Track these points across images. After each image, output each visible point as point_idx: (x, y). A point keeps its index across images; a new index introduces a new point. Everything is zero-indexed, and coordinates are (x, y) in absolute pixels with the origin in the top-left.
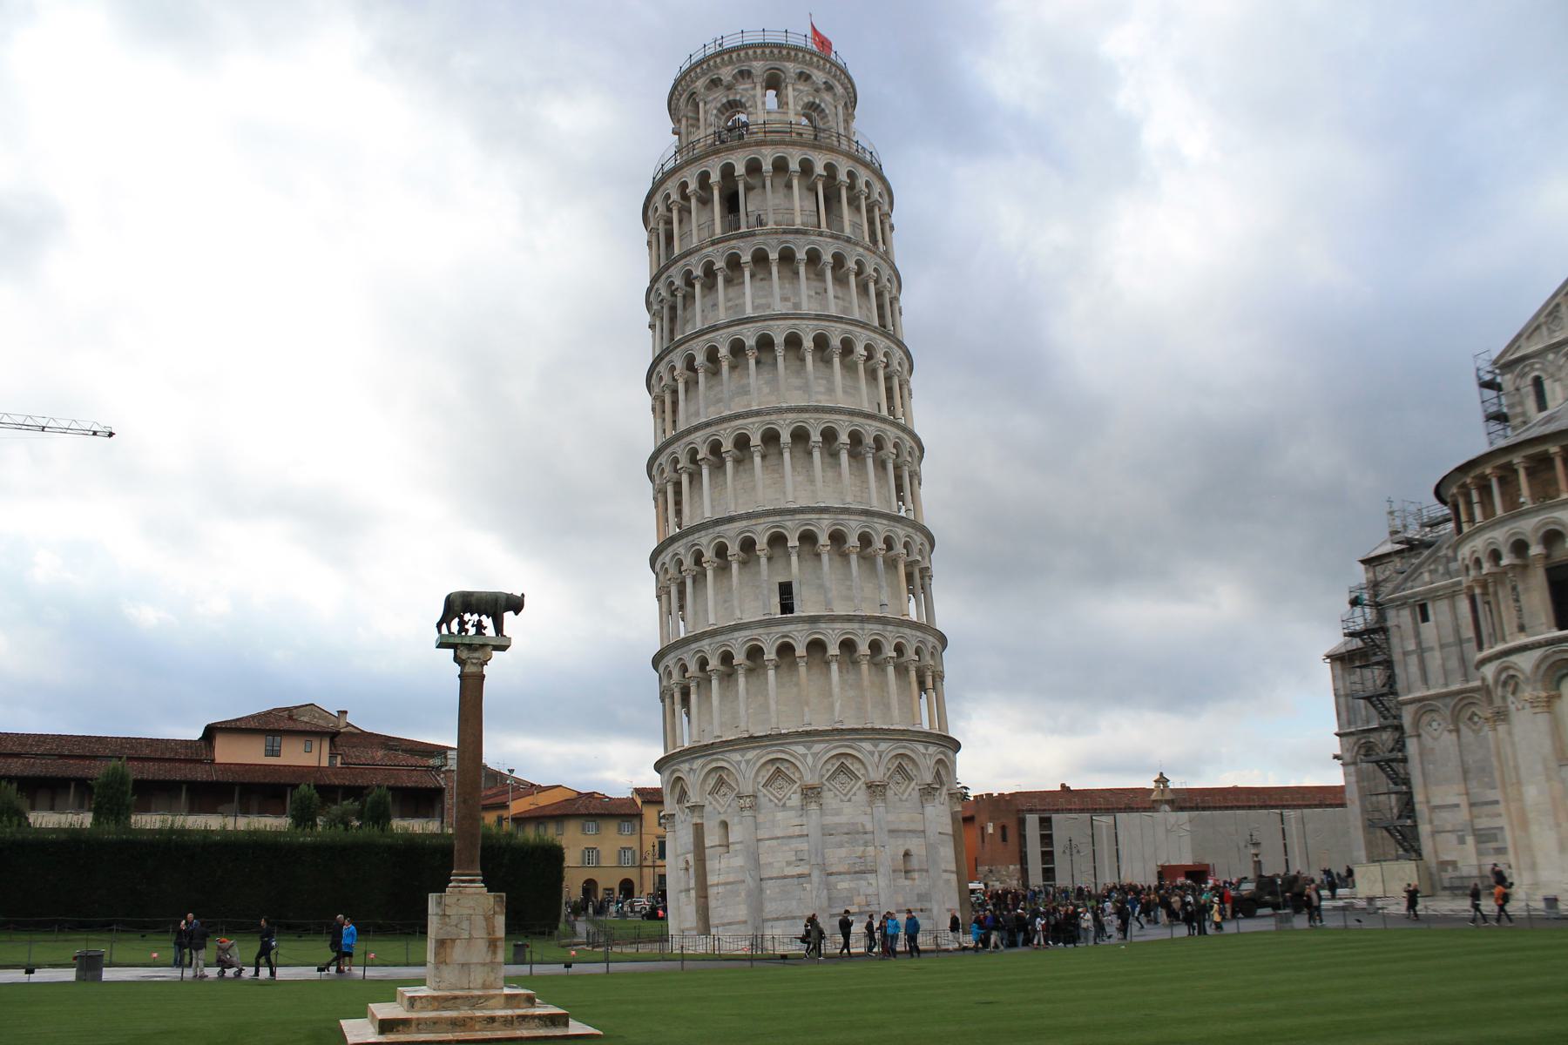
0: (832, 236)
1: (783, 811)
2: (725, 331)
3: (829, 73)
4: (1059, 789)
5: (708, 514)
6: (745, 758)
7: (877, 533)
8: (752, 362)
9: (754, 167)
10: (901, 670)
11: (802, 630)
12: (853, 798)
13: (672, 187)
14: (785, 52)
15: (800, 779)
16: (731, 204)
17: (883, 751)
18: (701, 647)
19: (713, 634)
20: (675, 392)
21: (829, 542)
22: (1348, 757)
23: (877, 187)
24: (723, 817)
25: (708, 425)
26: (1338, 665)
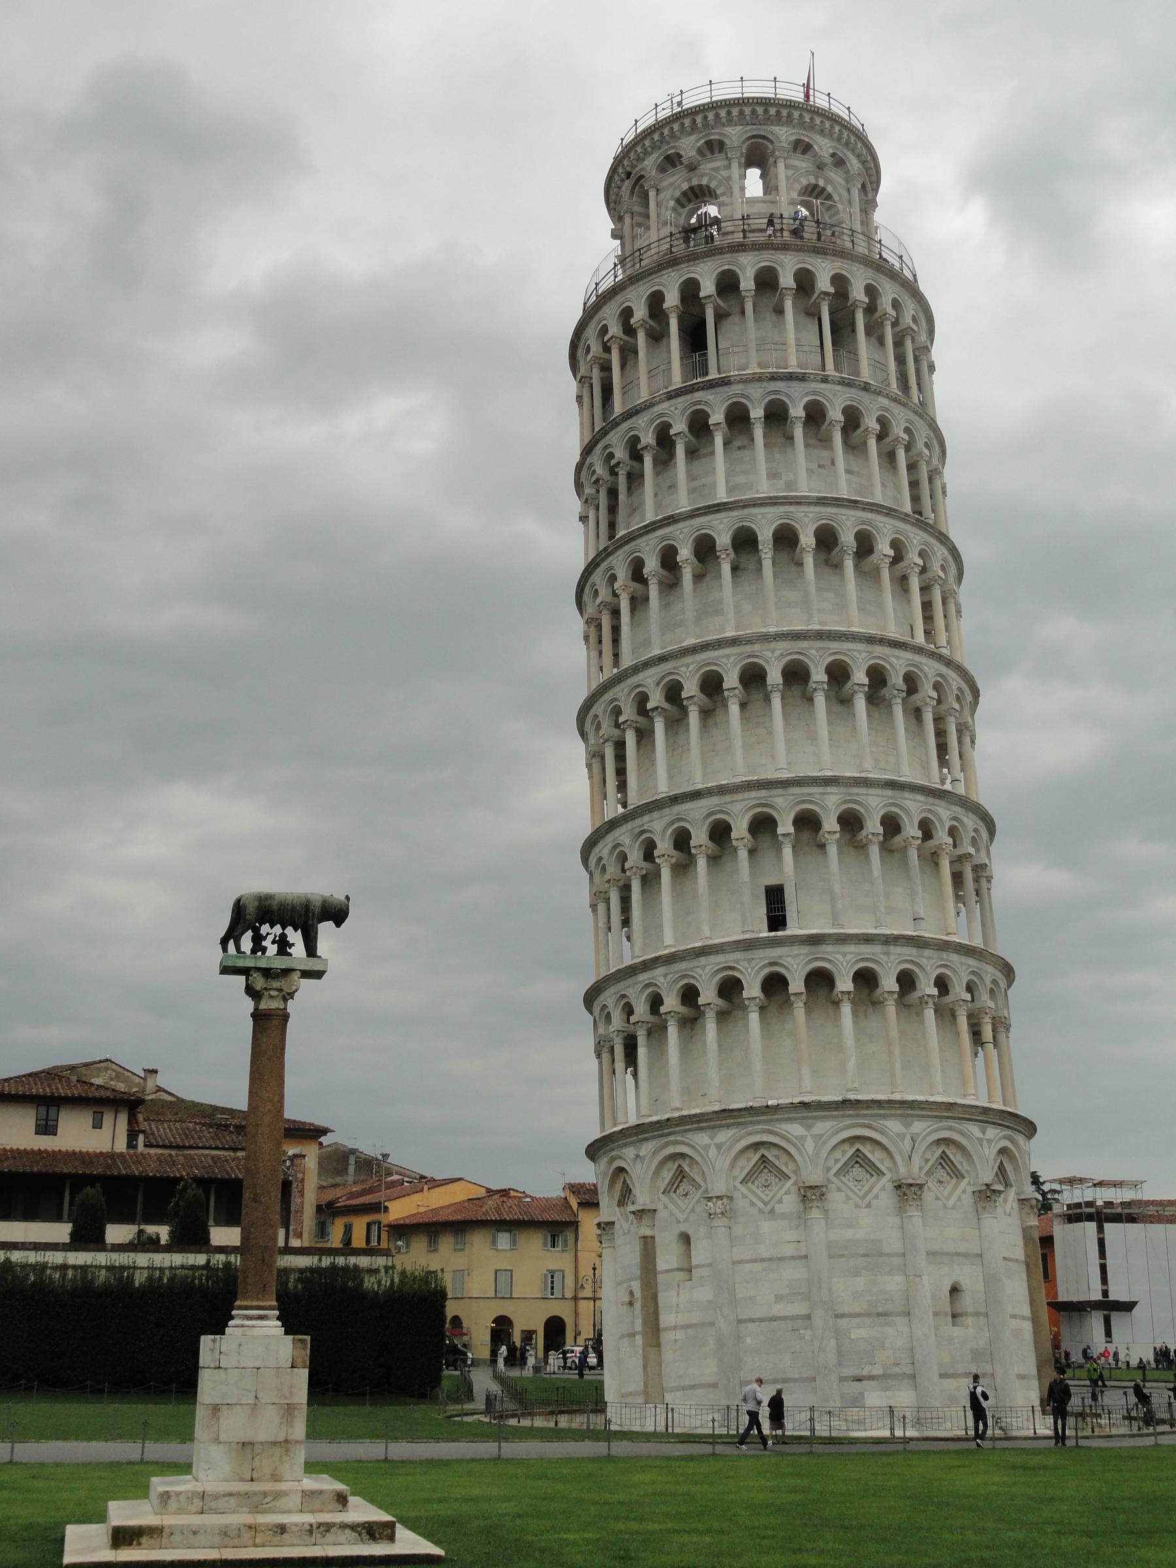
0: (843, 383)
1: (769, 1220)
3: (839, 139)
5: (663, 789)
8: (726, 568)
9: (728, 285)
10: (946, 1015)
11: (799, 955)
12: (874, 1202)
13: (610, 316)
14: (772, 111)
15: (795, 1172)
16: (695, 339)
17: (918, 1135)
18: (653, 978)
19: (671, 959)
20: (616, 613)
21: (837, 827)
23: (910, 308)
24: (683, 1228)
25: (662, 659)
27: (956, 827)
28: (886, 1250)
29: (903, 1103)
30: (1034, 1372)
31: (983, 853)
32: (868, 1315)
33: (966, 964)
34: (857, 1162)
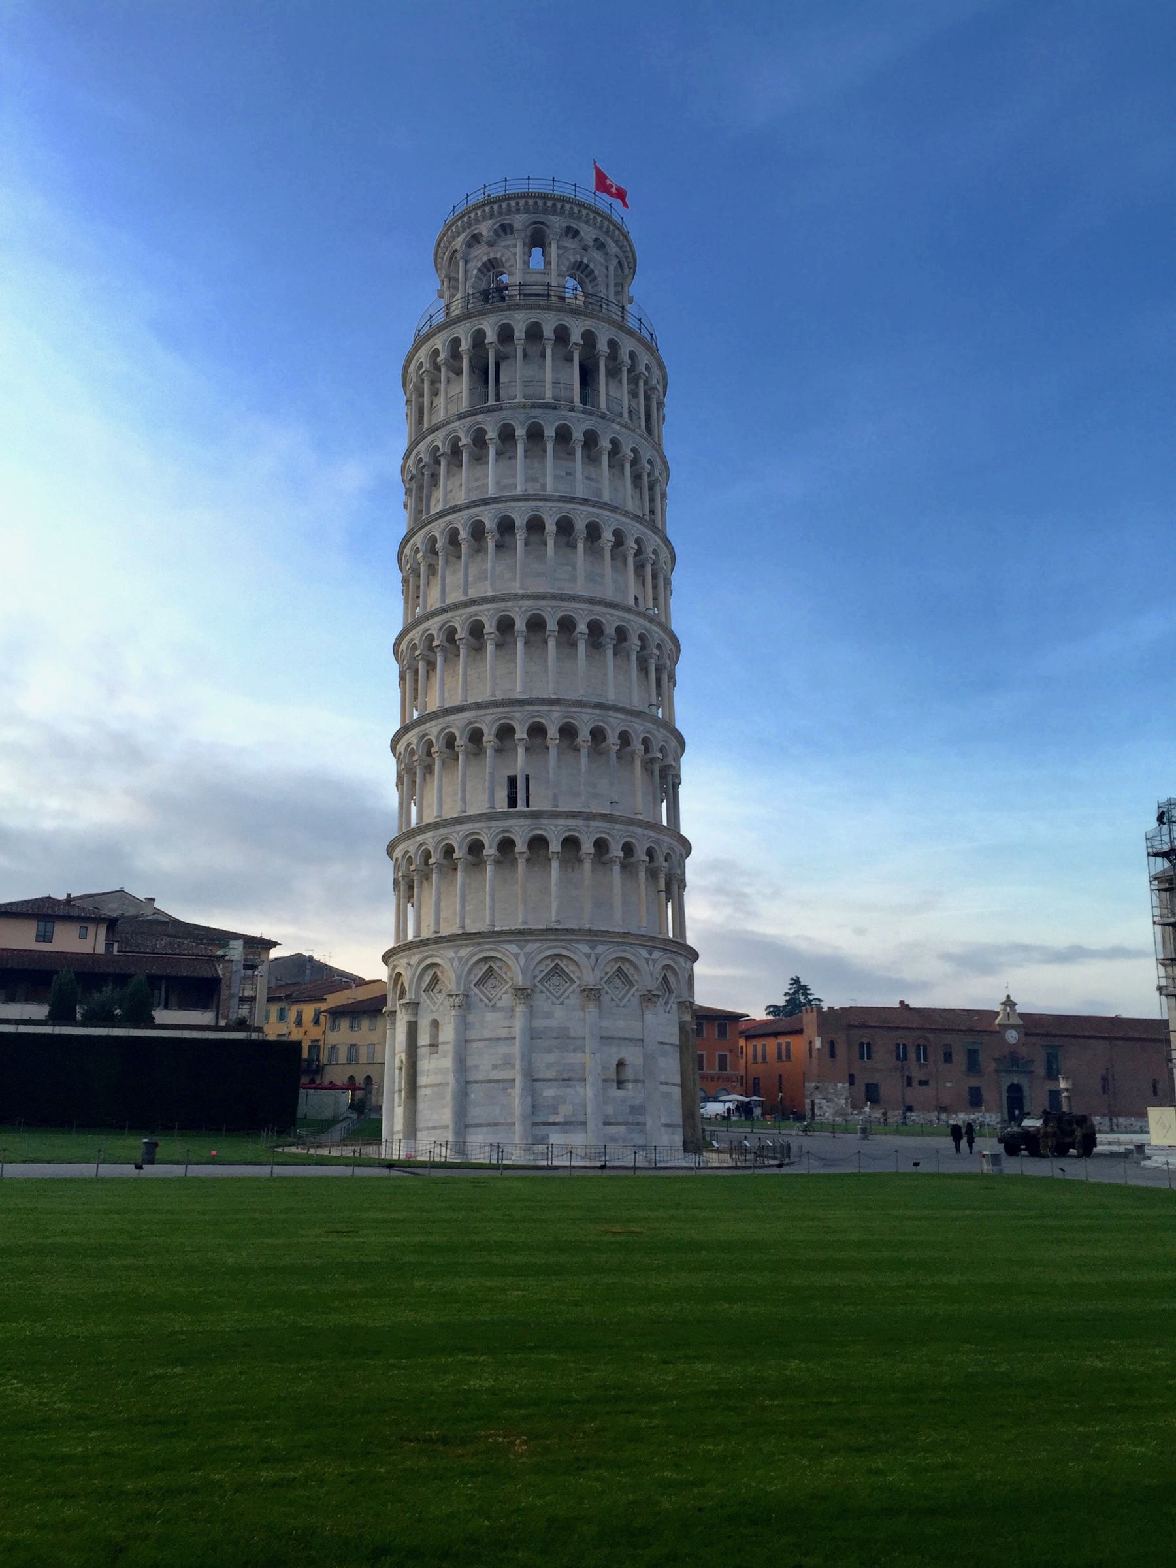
1: (492, 1011)
2: (467, 512)
3: (601, 228)
6: (524, 950)
9: (506, 334)
12: (566, 1001)
14: (550, 203)
16: (480, 372)
17: (601, 955)
21: (558, 735)
24: (435, 1016)
27: (649, 738)
28: (572, 1034)
30: (680, 1122)
31: (671, 757)
32: (555, 1080)
33: (647, 835)
34: (556, 973)
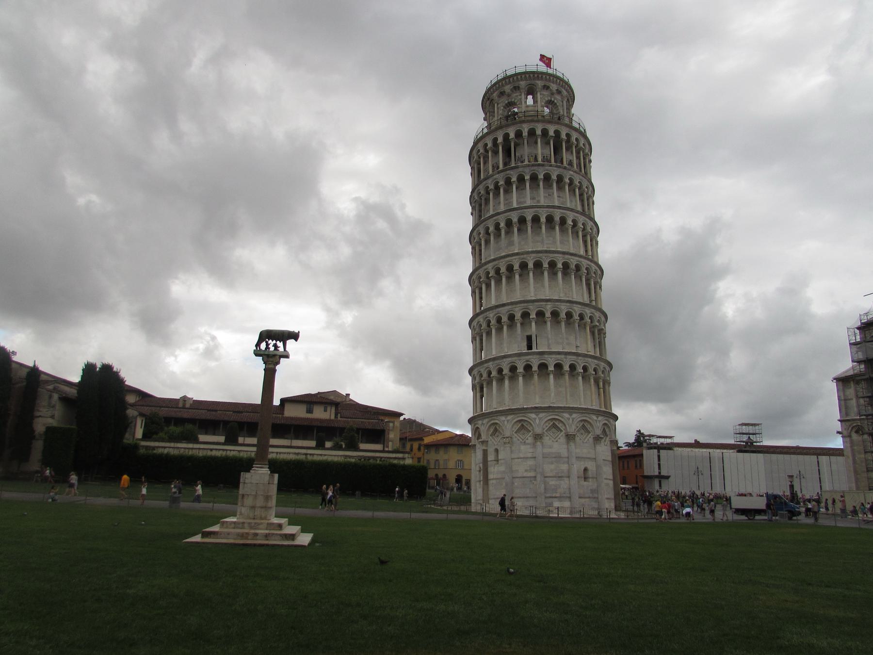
0: (557, 166)
3: (559, 85)
4: (694, 442)
5: (493, 302)
7: (575, 311)
8: (516, 230)
9: (519, 134)
13: (480, 146)
14: (536, 76)
16: (507, 152)
19: (494, 359)
20: (480, 245)
22: (845, 433)
23: (582, 141)
24: (496, 447)
25: (494, 260)
26: (840, 383)
29: (569, 408)
32: (555, 477)
